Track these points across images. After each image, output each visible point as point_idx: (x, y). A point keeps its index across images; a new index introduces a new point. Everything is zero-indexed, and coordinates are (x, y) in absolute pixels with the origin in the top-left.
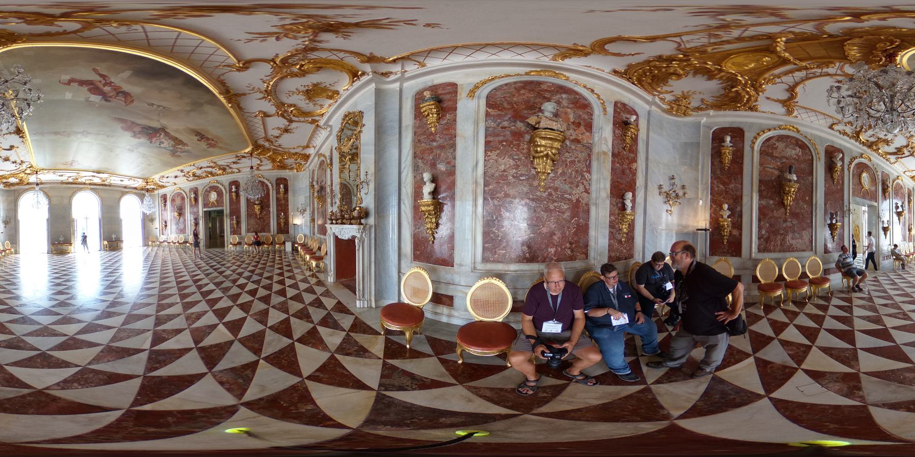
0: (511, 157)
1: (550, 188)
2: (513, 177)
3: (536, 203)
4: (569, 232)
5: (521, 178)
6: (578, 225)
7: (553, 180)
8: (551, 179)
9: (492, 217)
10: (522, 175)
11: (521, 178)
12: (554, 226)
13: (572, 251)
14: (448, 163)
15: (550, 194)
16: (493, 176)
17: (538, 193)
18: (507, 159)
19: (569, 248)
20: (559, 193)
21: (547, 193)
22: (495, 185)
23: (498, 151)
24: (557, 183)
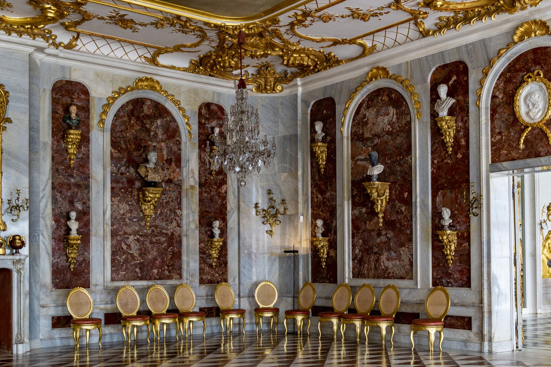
0: (127, 202)
1: (152, 226)
2: (129, 219)
3: (144, 238)
4: (167, 258)
5: (134, 220)
6: (173, 252)
7: (155, 220)
8: (153, 219)
9: (116, 248)
10: (135, 218)
11: (134, 220)
12: (156, 254)
13: (169, 272)
14: (84, 203)
15: (153, 231)
16: (116, 218)
17: (145, 231)
18: (124, 205)
19: (167, 270)
20: (159, 229)
21: (151, 231)
22: (117, 225)
23: (119, 198)
24: (158, 222)
